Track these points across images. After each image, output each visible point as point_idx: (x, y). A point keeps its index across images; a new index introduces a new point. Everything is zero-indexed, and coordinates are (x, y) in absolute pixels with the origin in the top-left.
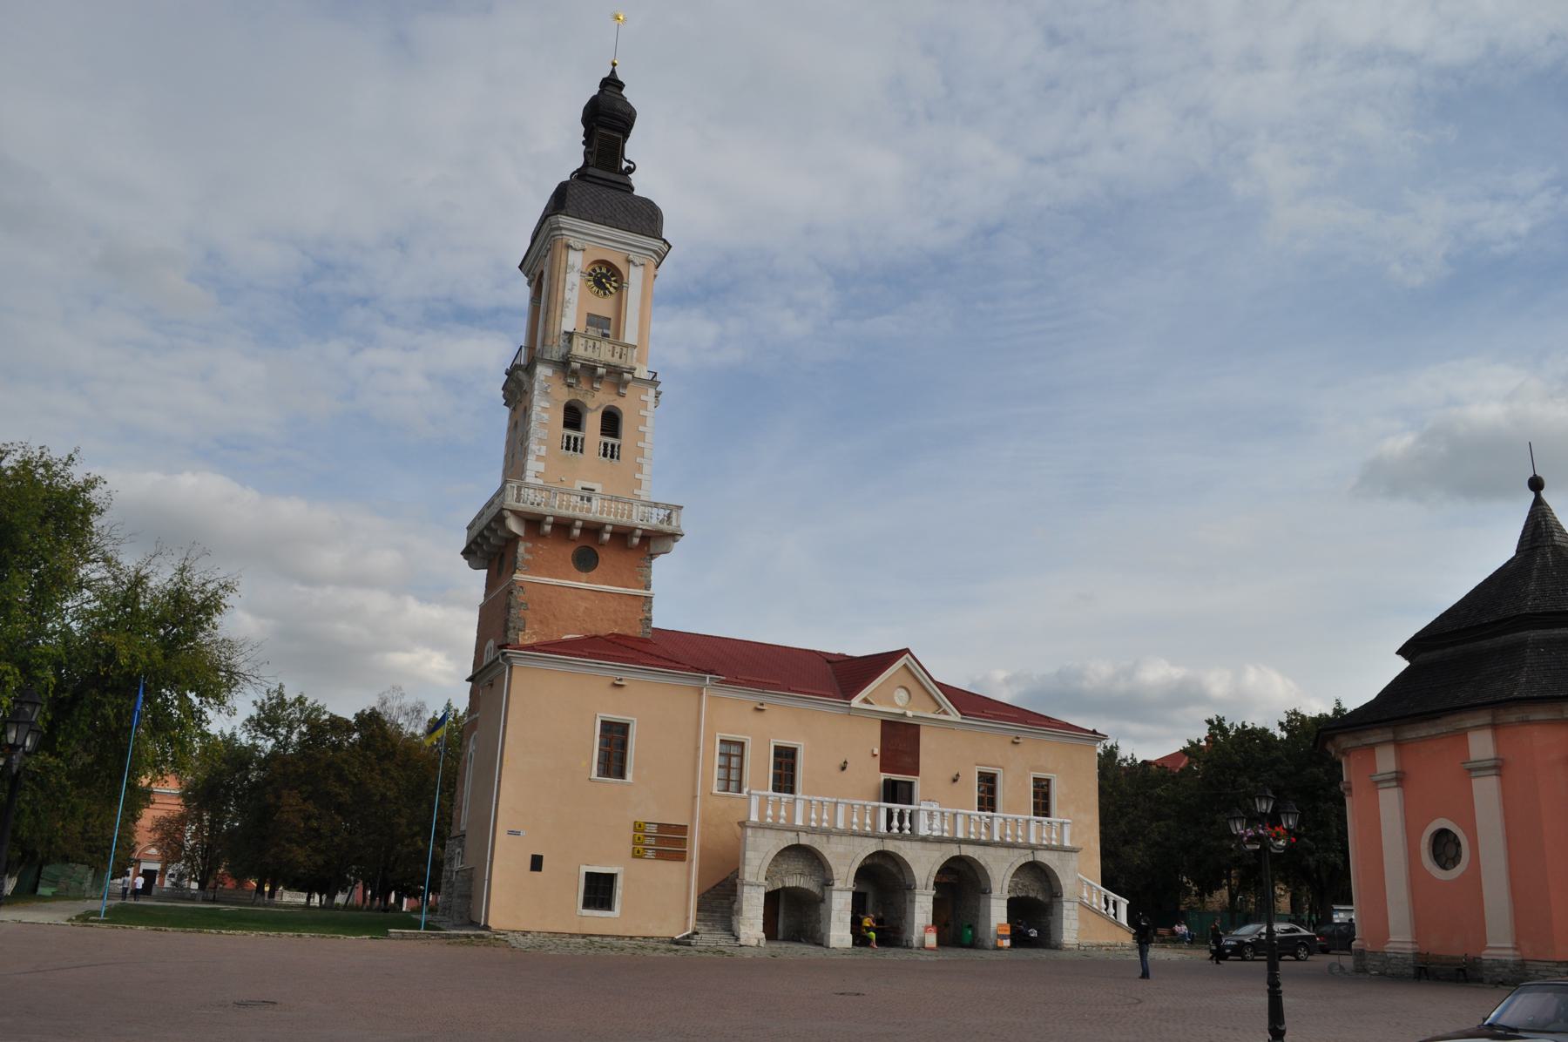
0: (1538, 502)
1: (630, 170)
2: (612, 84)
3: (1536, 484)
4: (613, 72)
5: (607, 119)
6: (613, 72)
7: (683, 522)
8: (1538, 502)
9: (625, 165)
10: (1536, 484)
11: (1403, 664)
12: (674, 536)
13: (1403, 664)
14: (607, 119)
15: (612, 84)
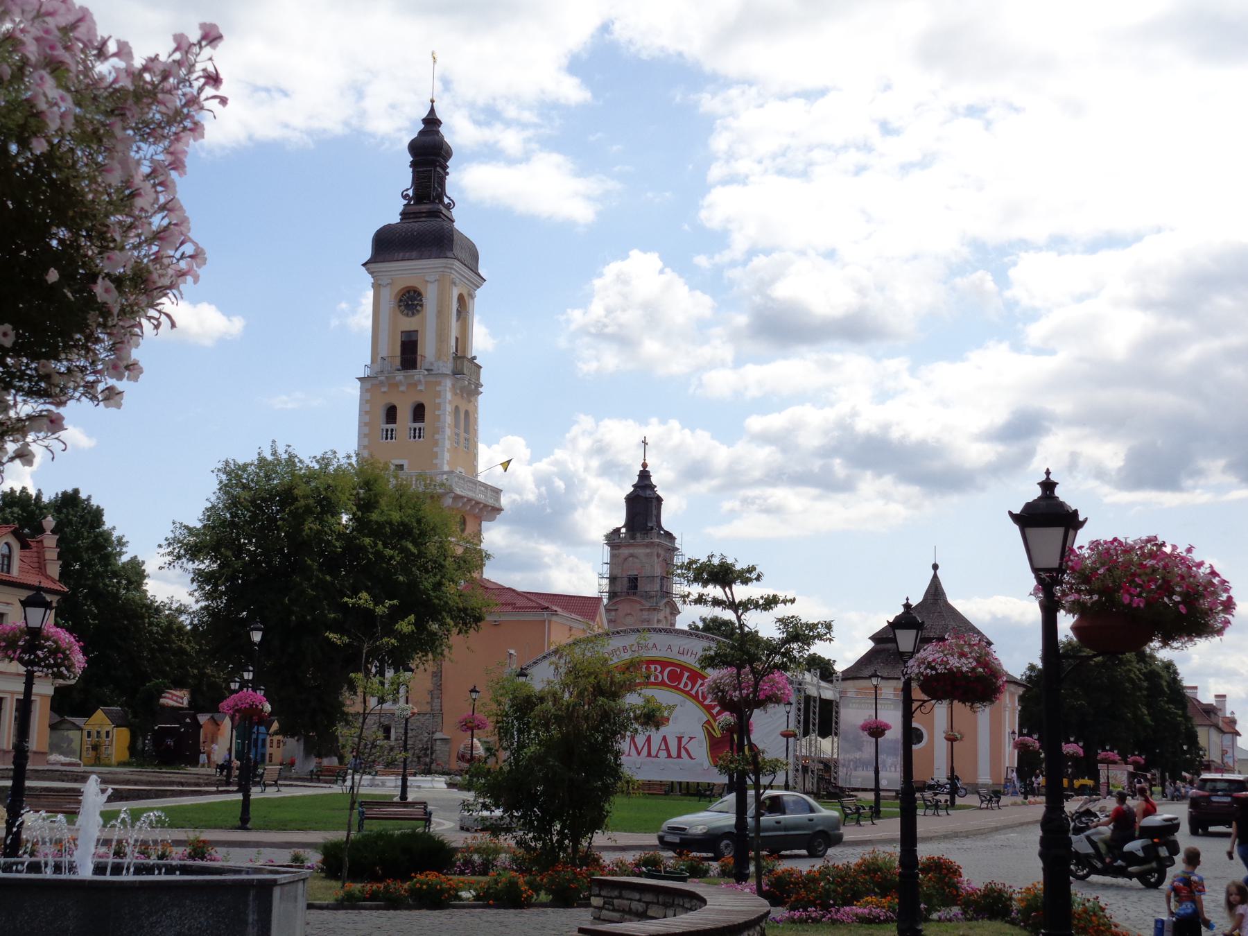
0: (935, 576)
1: (448, 207)
2: (432, 122)
3: (935, 567)
4: (432, 110)
5: (430, 153)
6: (432, 110)
7: (504, 501)
8: (935, 576)
9: (446, 201)
10: (935, 567)
11: (871, 645)
12: (499, 510)
13: (871, 645)
14: (430, 153)
15: (432, 122)
